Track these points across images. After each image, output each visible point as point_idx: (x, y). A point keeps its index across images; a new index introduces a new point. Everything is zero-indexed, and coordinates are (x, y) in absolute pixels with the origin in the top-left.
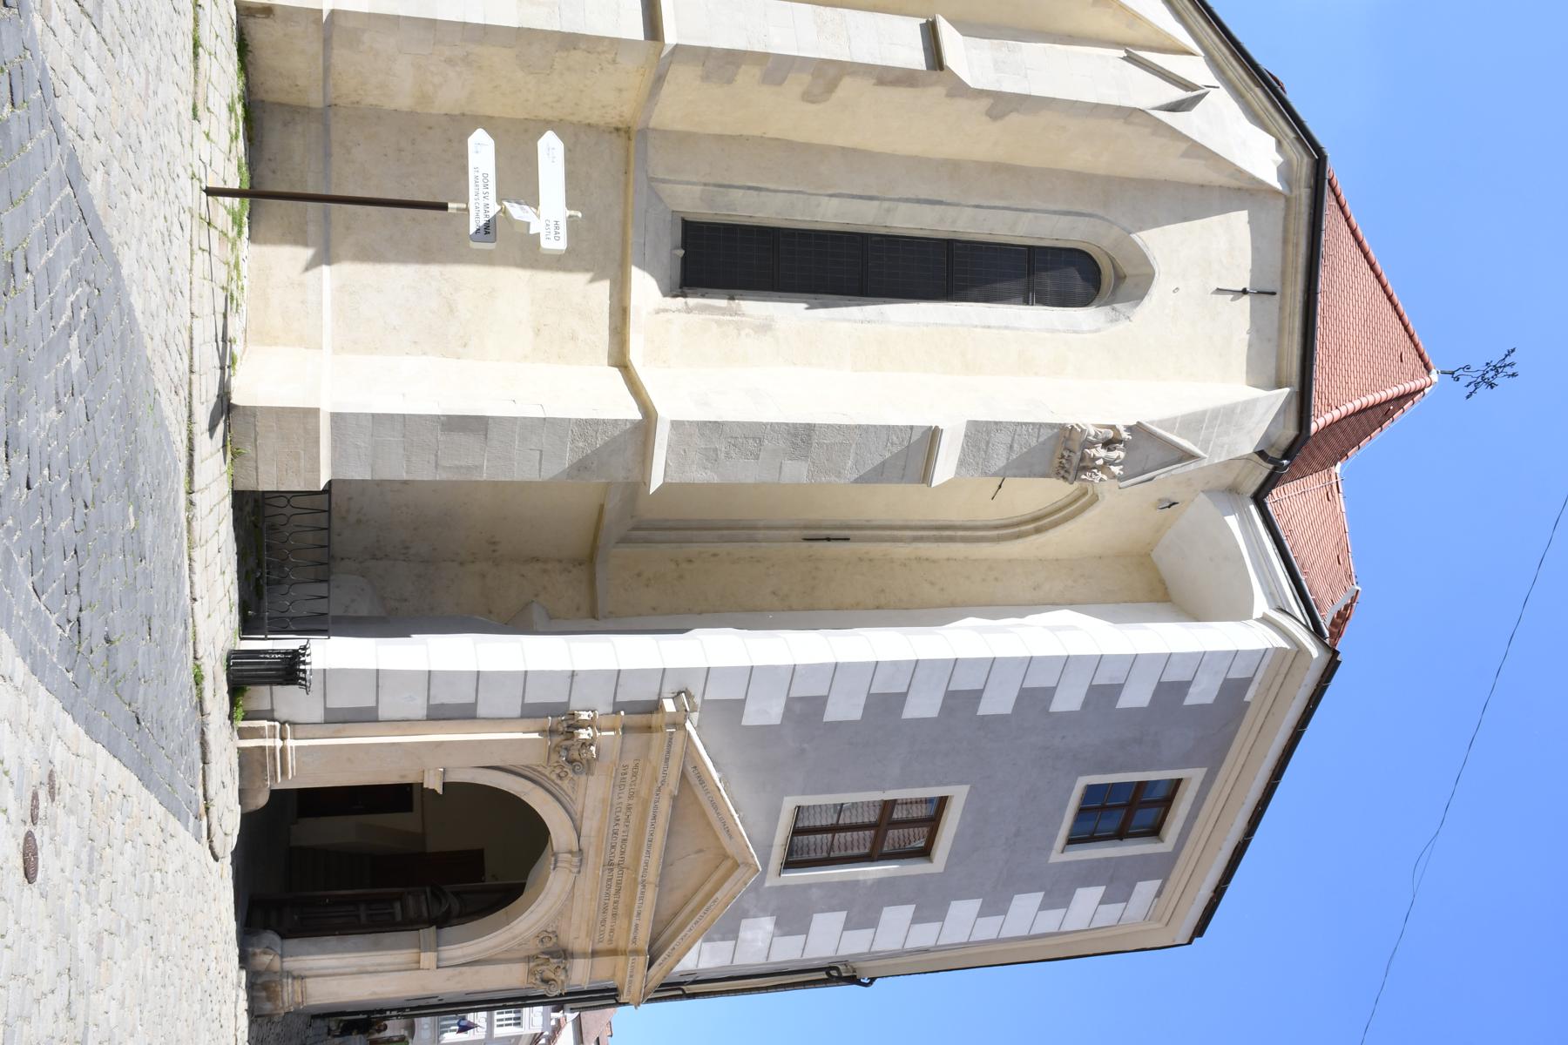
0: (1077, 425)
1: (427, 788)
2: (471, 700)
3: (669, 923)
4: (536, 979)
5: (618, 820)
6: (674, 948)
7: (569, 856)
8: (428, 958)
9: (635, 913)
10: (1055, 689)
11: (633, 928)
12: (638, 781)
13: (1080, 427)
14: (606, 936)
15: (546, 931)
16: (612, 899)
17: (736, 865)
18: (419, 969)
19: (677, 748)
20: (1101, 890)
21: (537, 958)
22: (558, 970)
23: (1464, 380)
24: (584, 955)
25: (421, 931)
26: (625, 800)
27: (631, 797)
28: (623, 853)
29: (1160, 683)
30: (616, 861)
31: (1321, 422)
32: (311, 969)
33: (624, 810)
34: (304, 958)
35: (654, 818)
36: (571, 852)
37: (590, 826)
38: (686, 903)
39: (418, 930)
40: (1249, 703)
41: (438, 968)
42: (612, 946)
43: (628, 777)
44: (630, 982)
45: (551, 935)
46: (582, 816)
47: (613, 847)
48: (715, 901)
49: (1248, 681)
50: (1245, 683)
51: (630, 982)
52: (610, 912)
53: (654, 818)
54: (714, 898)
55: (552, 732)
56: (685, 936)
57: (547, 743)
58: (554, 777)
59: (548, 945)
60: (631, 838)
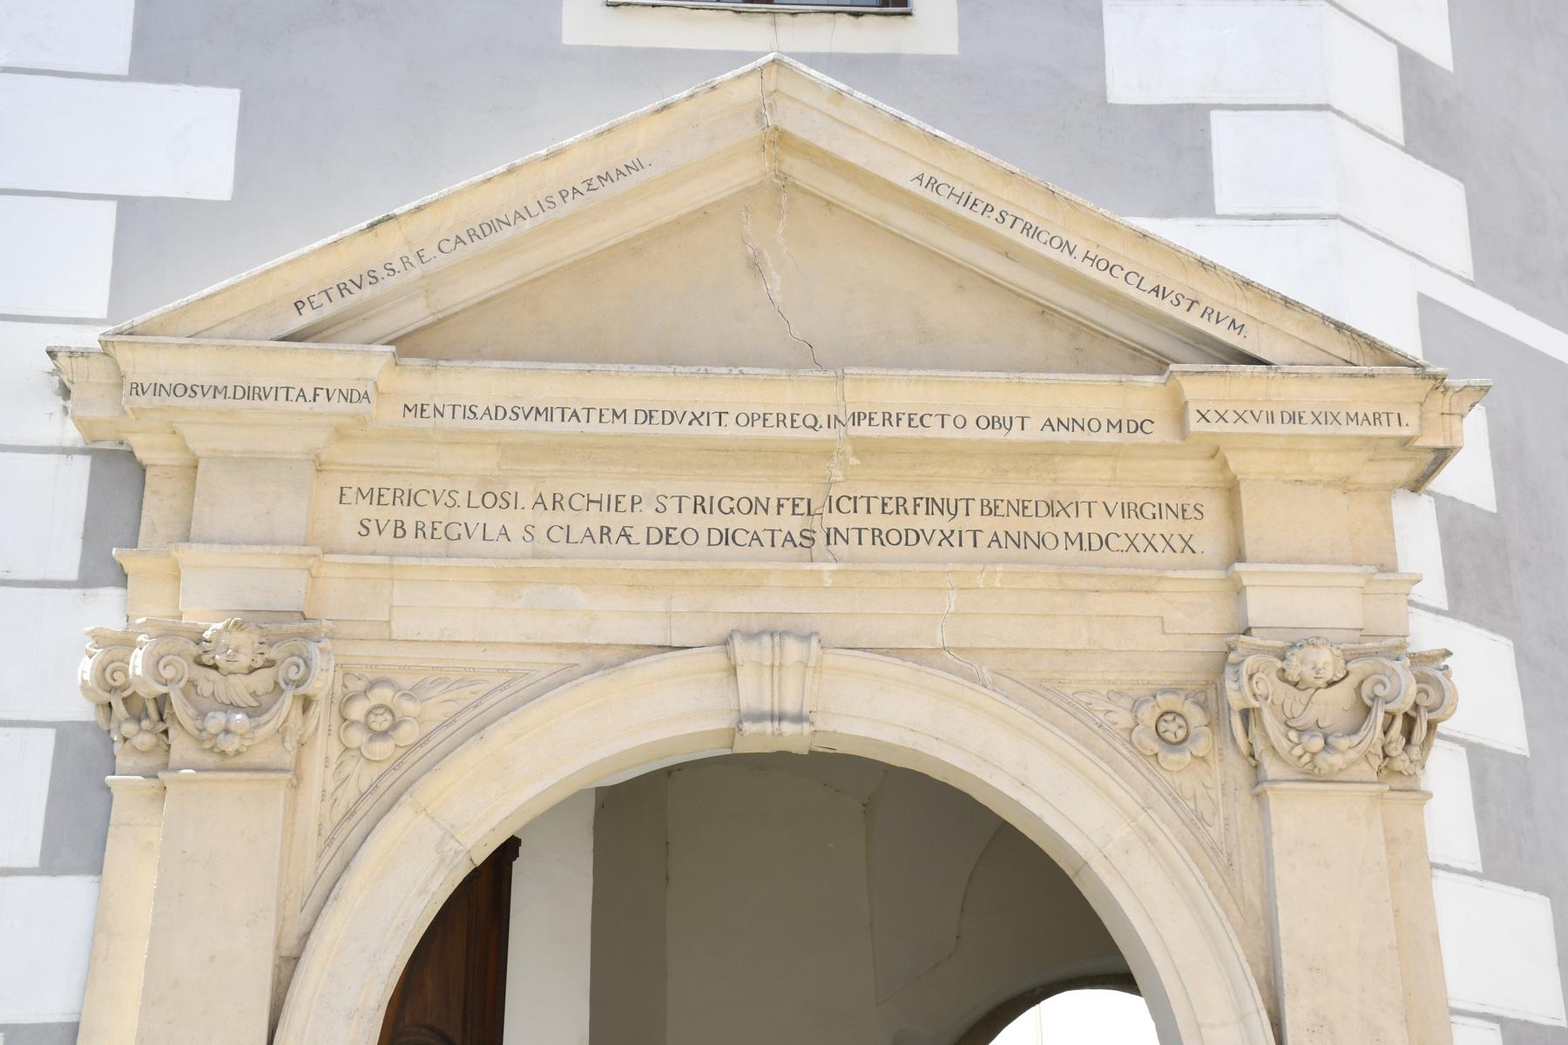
3: (1079, 327)
5: (605, 532)
6: (1156, 290)
11: (1062, 435)
12: (439, 485)
17: (780, 140)
27: (505, 501)
28: (755, 505)
33: (562, 517)
35: (547, 413)
43: (410, 516)
46: (583, 647)
47: (727, 537)
48: (933, 184)
52: (1044, 525)
53: (547, 413)
54: (915, 188)
55: (160, 766)
56: (1095, 261)
57: (189, 780)
58: (382, 749)
60: (692, 488)
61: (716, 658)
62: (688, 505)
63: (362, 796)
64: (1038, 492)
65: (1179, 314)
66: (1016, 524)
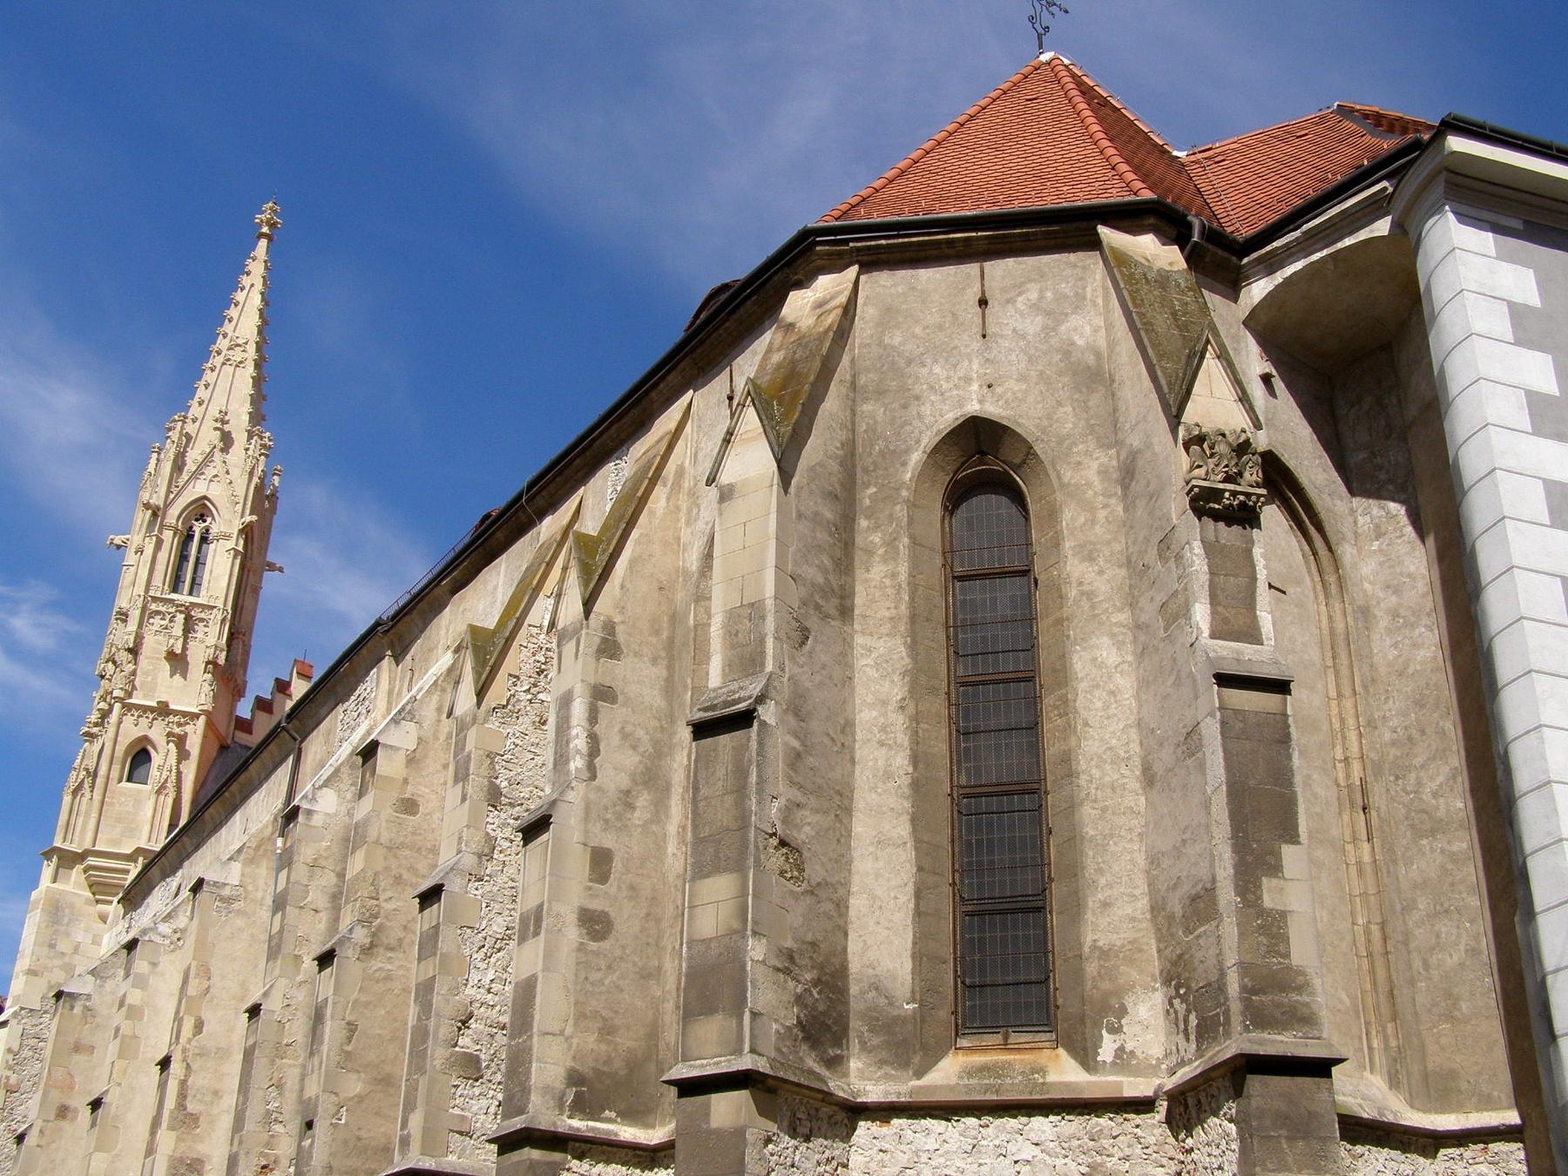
0: (1188, 494)
10: (1545, 481)
23: (1046, 19)
29: (1518, 342)
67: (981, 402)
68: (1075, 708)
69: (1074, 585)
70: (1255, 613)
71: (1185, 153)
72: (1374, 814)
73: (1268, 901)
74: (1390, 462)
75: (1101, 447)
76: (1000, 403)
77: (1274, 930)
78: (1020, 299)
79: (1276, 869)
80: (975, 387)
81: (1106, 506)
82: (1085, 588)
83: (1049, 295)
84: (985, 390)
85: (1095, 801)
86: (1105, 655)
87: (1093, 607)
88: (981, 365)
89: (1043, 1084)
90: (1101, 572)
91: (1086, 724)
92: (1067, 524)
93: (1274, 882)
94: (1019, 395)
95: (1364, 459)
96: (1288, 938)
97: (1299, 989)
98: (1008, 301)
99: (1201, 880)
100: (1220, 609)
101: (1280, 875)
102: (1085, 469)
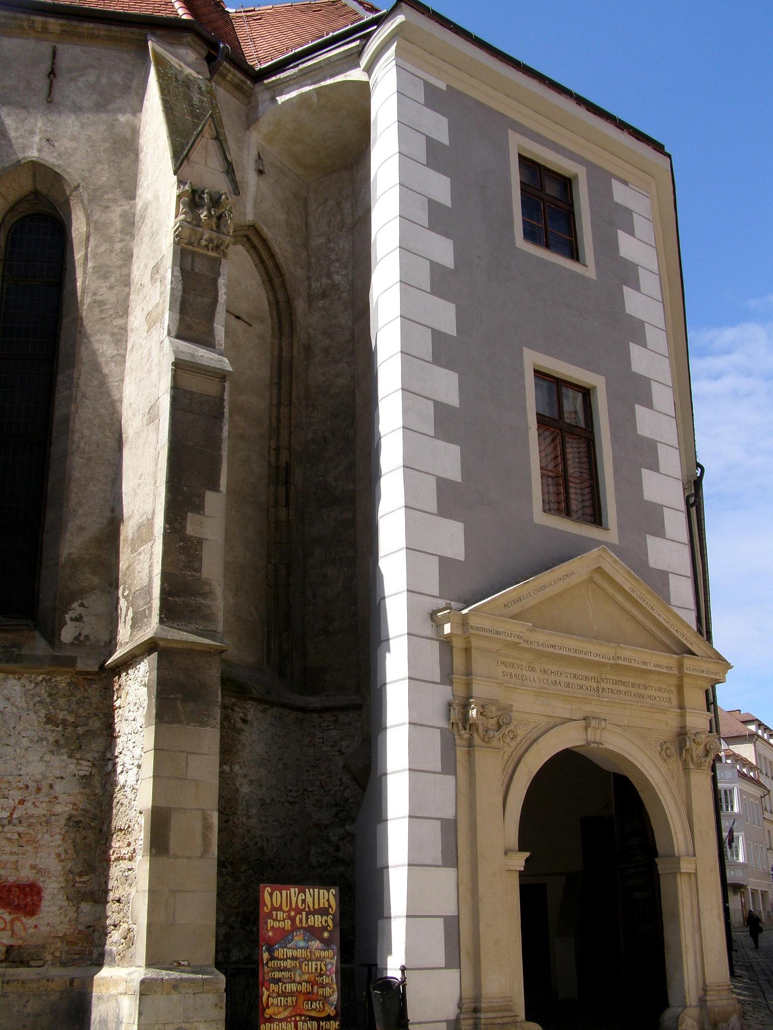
0: (175, 232)
1: (525, 867)
2: (438, 824)
4: (705, 761)
5: (556, 682)
7: (589, 730)
8: (686, 866)
9: (644, 667)
10: (432, 262)
12: (519, 662)
13: (178, 229)
14: (665, 695)
15: (660, 753)
16: (630, 689)
18: (696, 874)
19: (486, 623)
20: (620, 233)
21: (685, 761)
22: (697, 740)
24: (683, 716)
25: (660, 872)
26: (537, 675)
27: (533, 670)
29: (429, 165)
30: (595, 685)
31: (181, 12)
32: (697, 977)
33: (545, 676)
34: (686, 984)
36: (586, 728)
37: (561, 710)
38: (634, 618)
39: (658, 875)
40: (448, 86)
41: (695, 856)
42: (674, 689)
43: (514, 671)
44: (708, 672)
45: (665, 747)
46: (552, 717)
47: (581, 687)
48: (633, 591)
49: (427, 85)
50: (430, 89)
51: (708, 672)
52: (643, 692)
53: (554, 646)
54: (628, 590)
58: (514, 744)
59: (673, 750)
61: (583, 723)
62: (572, 676)
63: (509, 758)
64: (642, 682)
65: (680, 638)
66: (638, 691)
67: (39, 151)
68: (78, 384)
69: (90, 295)
70: (213, 325)
71: (234, 11)
72: (292, 488)
73: (190, 530)
74: (339, 247)
75: (125, 198)
76: (55, 154)
77: (192, 551)
78: (81, 79)
79: (199, 508)
80: (37, 139)
81: (122, 240)
82: (98, 298)
83: (104, 80)
84: (44, 143)
85: (83, 453)
86: (105, 347)
87: (102, 311)
88: (44, 124)
89: (18, 655)
90: (111, 288)
91: (84, 396)
92: (92, 250)
93: (197, 516)
94: (70, 151)
95: (322, 243)
96: (201, 558)
97: (205, 595)
98: (72, 79)
99: (145, 513)
100: (187, 318)
101: (202, 512)
102: (111, 212)
